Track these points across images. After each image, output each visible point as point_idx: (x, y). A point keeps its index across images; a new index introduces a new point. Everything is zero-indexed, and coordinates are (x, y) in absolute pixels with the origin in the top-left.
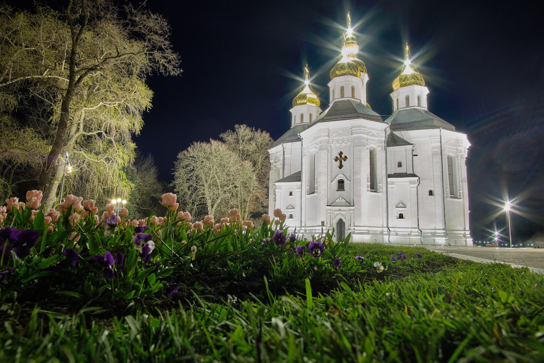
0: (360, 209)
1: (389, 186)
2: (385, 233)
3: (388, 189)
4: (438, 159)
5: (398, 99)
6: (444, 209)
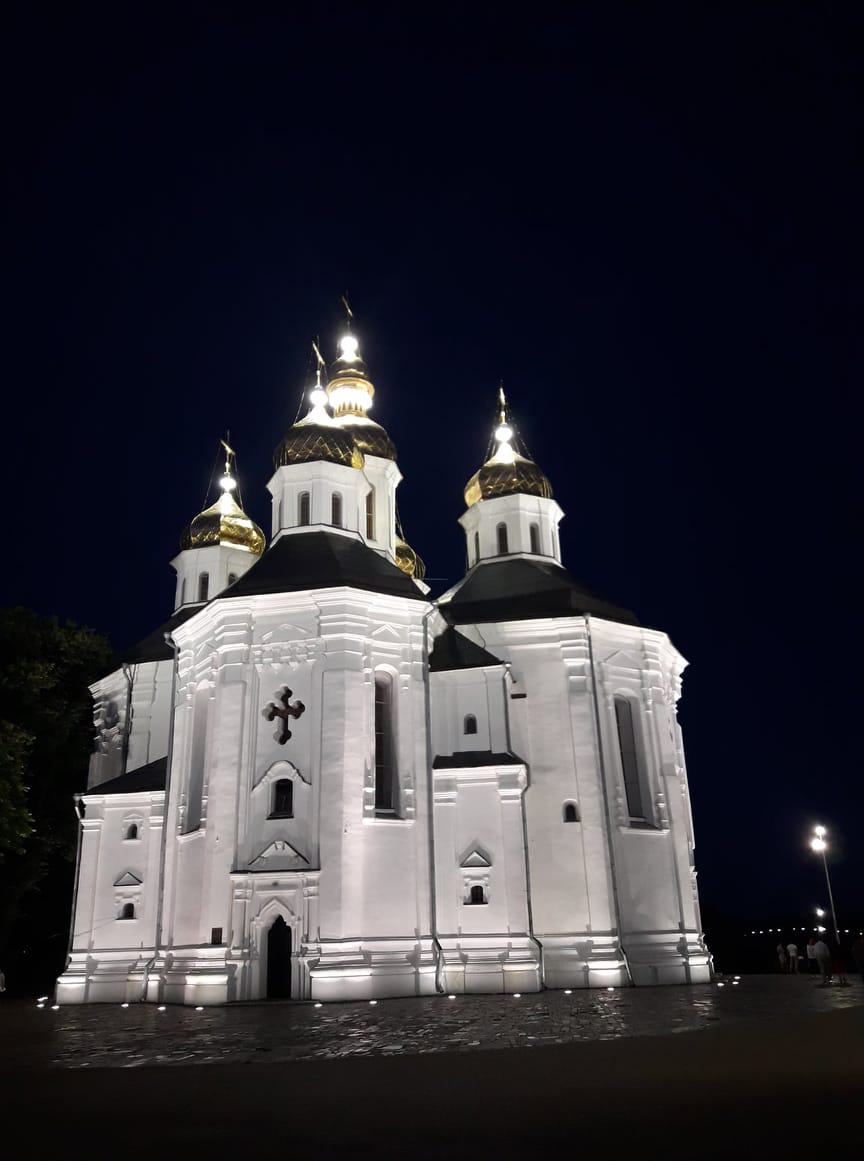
0: (337, 879)
1: (436, 795)
2: (424, 957)
3: (435, 805)
4: (583, 707)
5: (477, 534)
6: (612, 864)
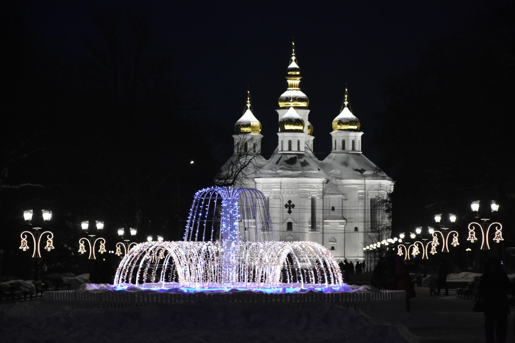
1: (325, 226)
4: (361, 203)
